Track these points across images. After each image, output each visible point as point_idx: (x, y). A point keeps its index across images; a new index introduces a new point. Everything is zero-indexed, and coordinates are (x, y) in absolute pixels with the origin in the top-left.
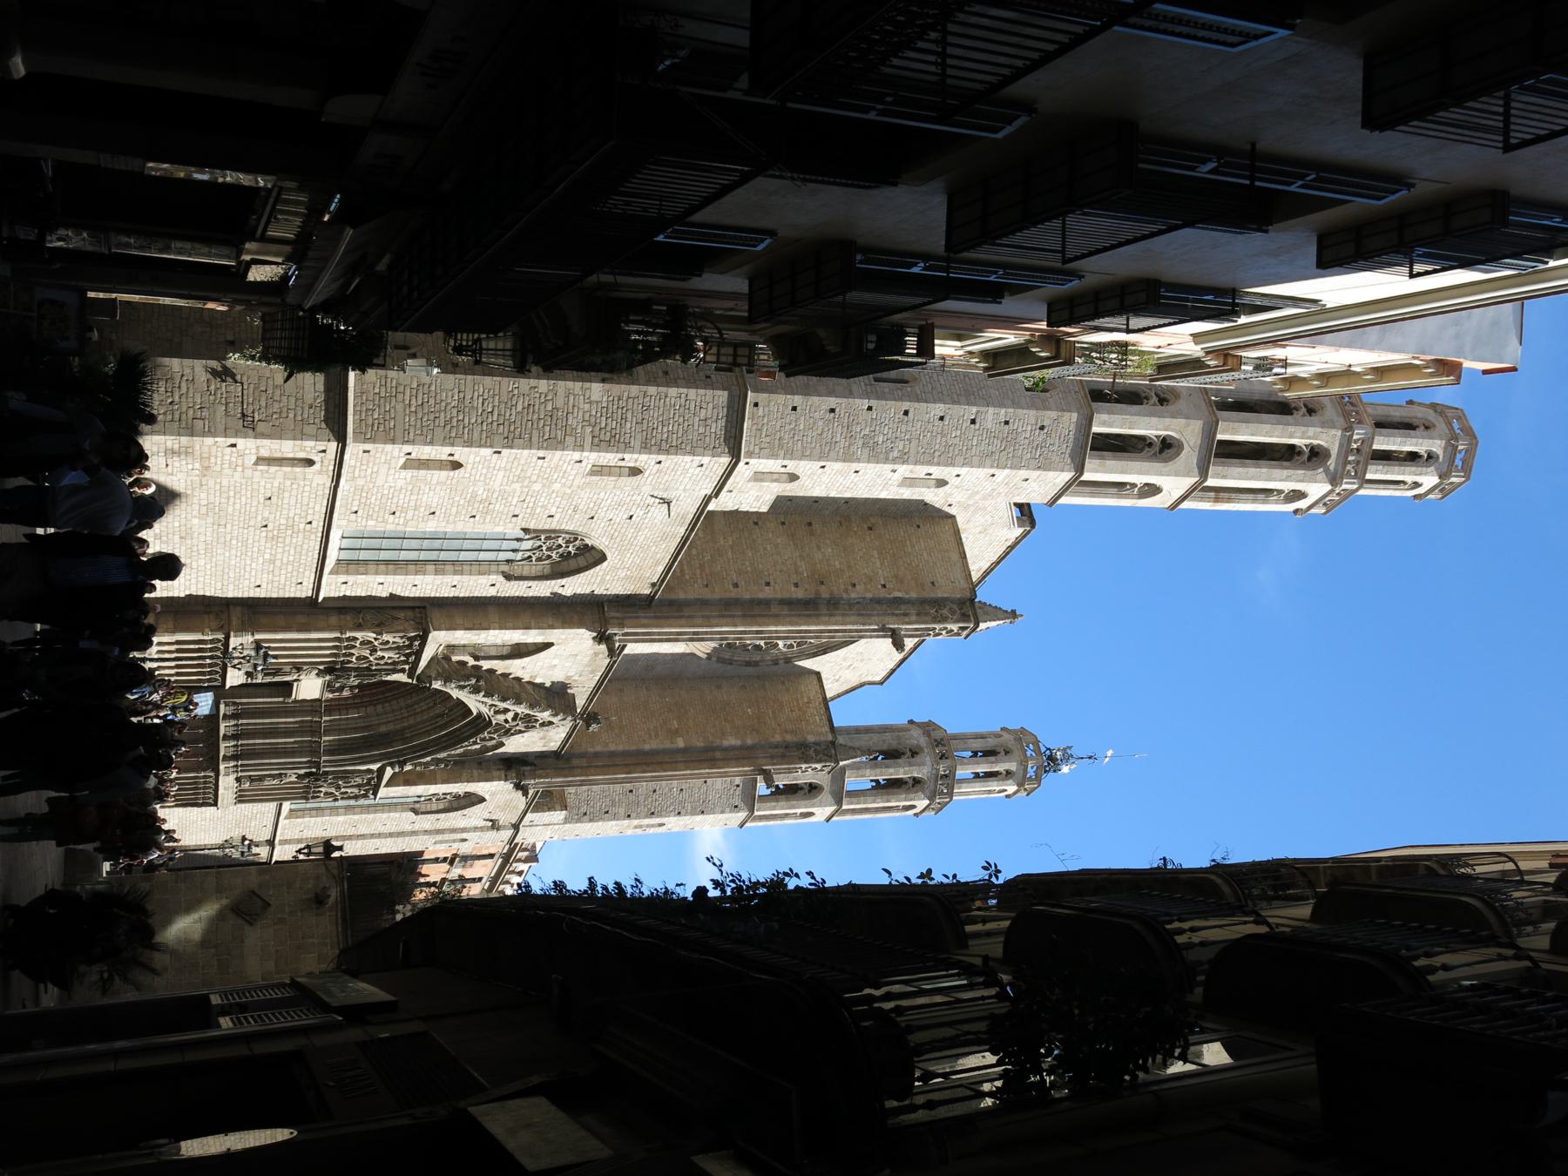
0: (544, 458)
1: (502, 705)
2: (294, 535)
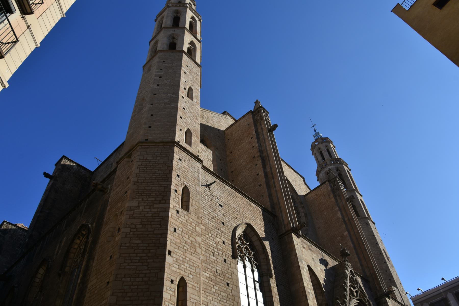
1: (348, 290)
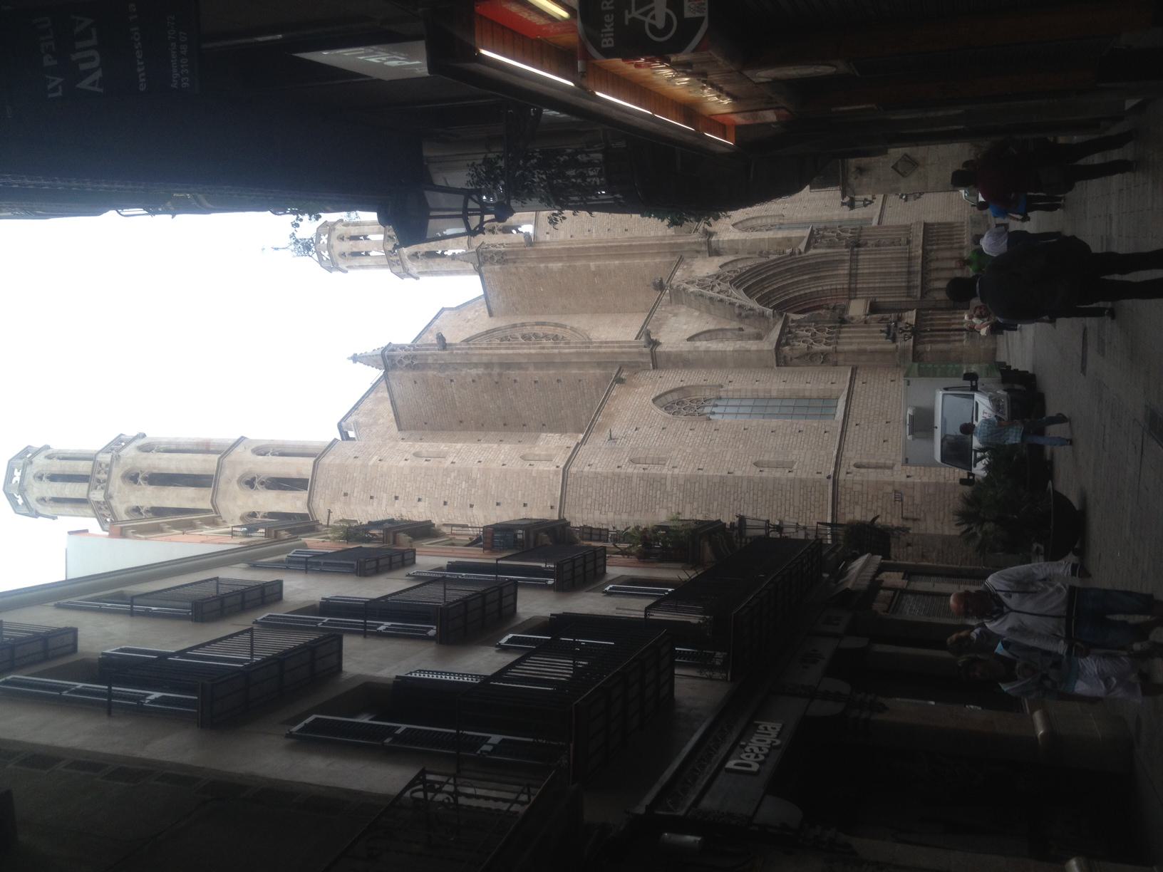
0: (699, 469)
1: (722, 296)
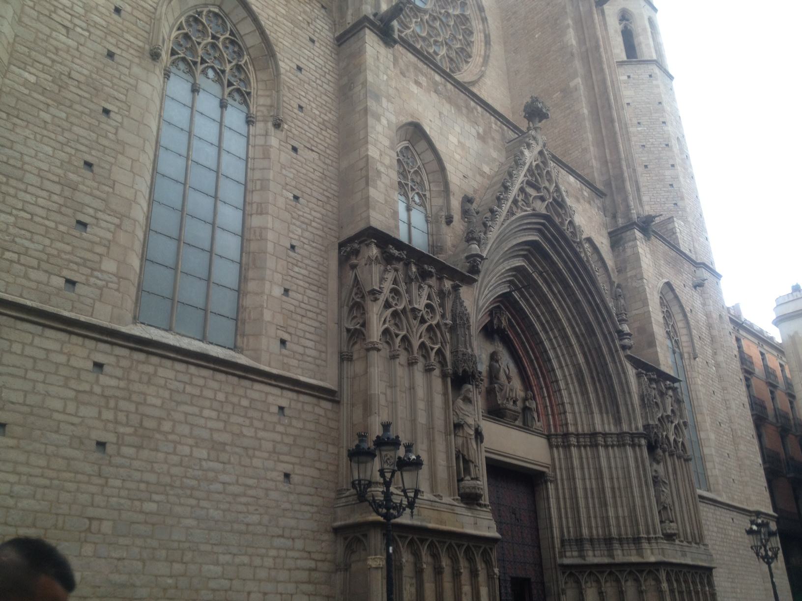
2: (135, 397)
